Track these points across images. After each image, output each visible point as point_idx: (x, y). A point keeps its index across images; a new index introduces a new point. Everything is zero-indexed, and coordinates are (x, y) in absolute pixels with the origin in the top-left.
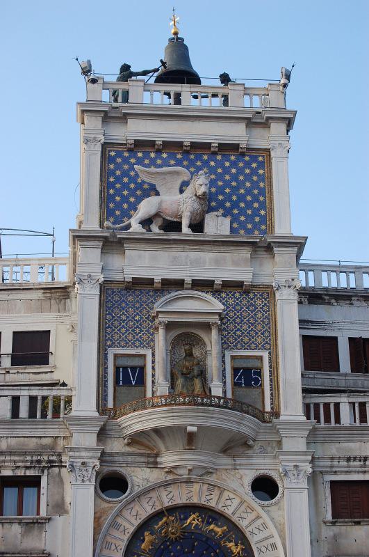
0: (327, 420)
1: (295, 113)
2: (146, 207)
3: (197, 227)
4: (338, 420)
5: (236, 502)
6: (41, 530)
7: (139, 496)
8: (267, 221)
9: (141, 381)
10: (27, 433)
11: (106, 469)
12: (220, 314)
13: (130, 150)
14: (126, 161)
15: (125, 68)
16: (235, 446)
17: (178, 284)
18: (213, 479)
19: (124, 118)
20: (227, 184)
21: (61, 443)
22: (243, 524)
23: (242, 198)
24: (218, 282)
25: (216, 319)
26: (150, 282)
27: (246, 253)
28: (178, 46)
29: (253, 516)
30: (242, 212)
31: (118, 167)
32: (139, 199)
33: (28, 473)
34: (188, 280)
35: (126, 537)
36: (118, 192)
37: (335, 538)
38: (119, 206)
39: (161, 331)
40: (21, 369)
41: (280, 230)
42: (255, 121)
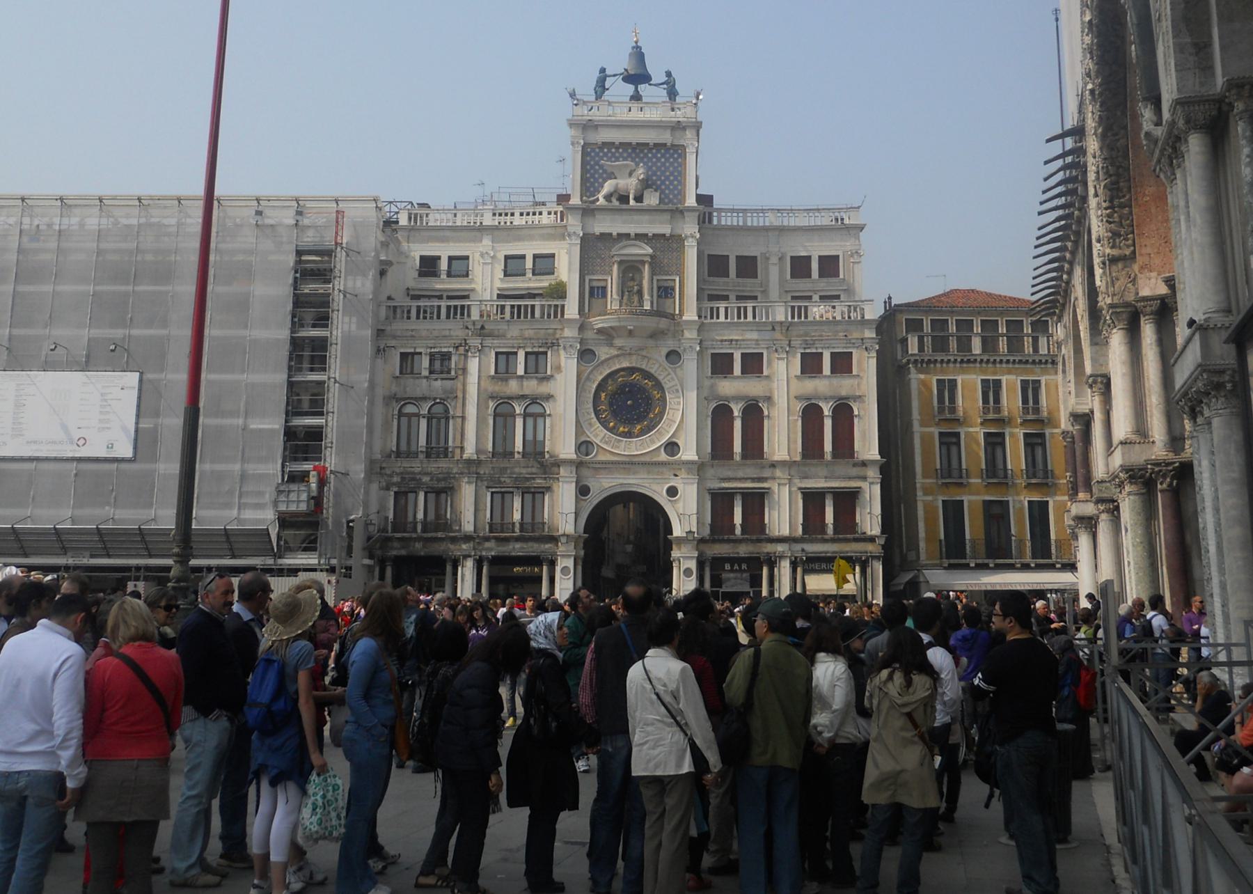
3: (639, 199)
9: (604, 295)
14: (597, 155)
15: (603, 70)
16: (655, 335)
17: (627, 236)
18: (644, 353)
19: (596, 127)
20: (659, 169)
22: (660, 378)
23: (667, 178)
26: (611, 234)
27: (667, 216)
28: (638, 55)
31: (593, 158)
32: (605, 181)
34: (633, 235)
36: (592, 176)
38: (592, 185)
42: (678, 127)
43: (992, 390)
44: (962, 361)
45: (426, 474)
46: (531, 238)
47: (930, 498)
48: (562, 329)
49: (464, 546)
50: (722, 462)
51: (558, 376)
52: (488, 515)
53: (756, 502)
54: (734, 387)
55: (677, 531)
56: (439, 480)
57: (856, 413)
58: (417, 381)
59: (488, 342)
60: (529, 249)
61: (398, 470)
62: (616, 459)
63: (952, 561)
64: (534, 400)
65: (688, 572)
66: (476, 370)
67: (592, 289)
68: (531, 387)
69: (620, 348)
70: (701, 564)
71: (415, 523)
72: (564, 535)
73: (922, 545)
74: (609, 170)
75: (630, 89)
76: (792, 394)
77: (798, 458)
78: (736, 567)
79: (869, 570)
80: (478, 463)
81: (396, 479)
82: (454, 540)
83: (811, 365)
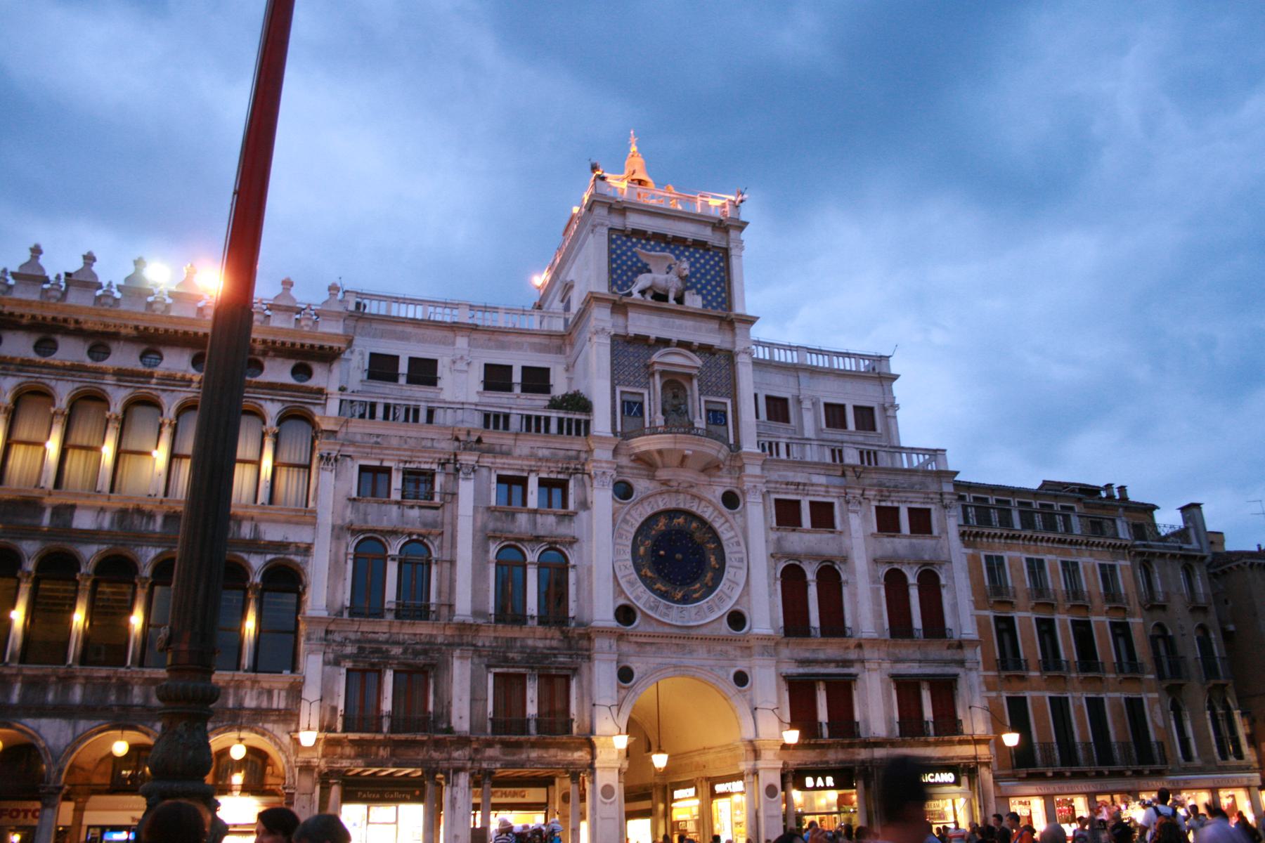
0: (771, 454)
1: (746, 223)
2: (643, 281)
3: (680, 300)
4: (778, 454)
5: (711, 509)
6: (570, 520)
7: (642, 500)
8: (728, 302)
9: (642, 414)
10: (558, 446)
13: (627, 236)
16: (710, 468)
17: (666, 343)
18: (694, 491)
21: (583, 456)
23: (708, 282)
24: (696, 344)
25: (695, 372)
27: (714, 325)
29: (722, 520)
30: (709, 293)
32: (636, 274)
33: (561, 476)
35: (633, 531)
37: (779, 540)
38: (620, 277)
39: (657, 377)
40: (529, 395)
41: (738, 309)
43: (1036, 567)
44: (1007, 537)
45: (397, 643)
46: (519, 347)
47: (994, 694)
48: (590, 451)
49: (456, 754)
50: (799, 640)
52: (490, 708)
56: (416, 654)
57: (943, 581)
58: (384, 507)
59: (487, 460)
60: (518, 359)
61: (352, 636)
62: (667, 630)
63: (1031, 770)
64: (552, 547)
66: (469, 500)
67: (623, 402)
68: (547, 524)
69: (665, 483)
70: (783, 777)
71: (380, 718)
74: (645, 260)
77: (887, 635)
78: (820, 782)
80: (475, 628)
81: (349, 649)
82: (438, 745)
83: (887, 521)
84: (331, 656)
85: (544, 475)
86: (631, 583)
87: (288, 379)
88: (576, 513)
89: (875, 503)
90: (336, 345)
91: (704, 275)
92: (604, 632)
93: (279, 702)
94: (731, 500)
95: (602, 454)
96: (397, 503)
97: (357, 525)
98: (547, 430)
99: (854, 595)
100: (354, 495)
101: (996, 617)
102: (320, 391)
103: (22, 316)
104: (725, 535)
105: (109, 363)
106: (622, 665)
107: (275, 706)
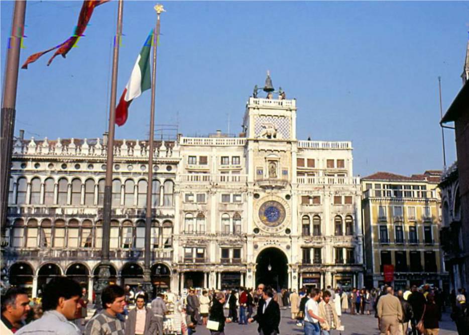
3: (275, 136)
11: (255, 193)
12: (280, 159)
15: (256, 86)
16: (280, 188)
47: (376, 250)
51: (245, 204)
53: (318, 251)
54: (311, 209)
55: (290, 262)
59: (219, 190)
65: (295, 277)
68: (236, 208)
69: (269, 193)
72: (251, 263)
73: (374, 267)
75: (266, 94)
76: (332, 211)
79: (359, 277)
83: (337, 200)
84: (180, 244)
85: (234, 193)
86: (259, 222)
87: (166, 171)
88: (243, 204)
89: (333, 195)
90: (177, 161)
91: (283, 127)
92: (250, 236)
93: (169, 256)
94: (288, 197)
95: (250, 186)
96: (196, 203)
97: (185, 210)
98: (236, 180)
99: (325, 224)
100: (185, 202)
101: (381, 226)
102: (174, 174)
103: (98, 160)
104: (286, 207)
105: (120, 170)
106: (255, 244)
107: (167, 257)
